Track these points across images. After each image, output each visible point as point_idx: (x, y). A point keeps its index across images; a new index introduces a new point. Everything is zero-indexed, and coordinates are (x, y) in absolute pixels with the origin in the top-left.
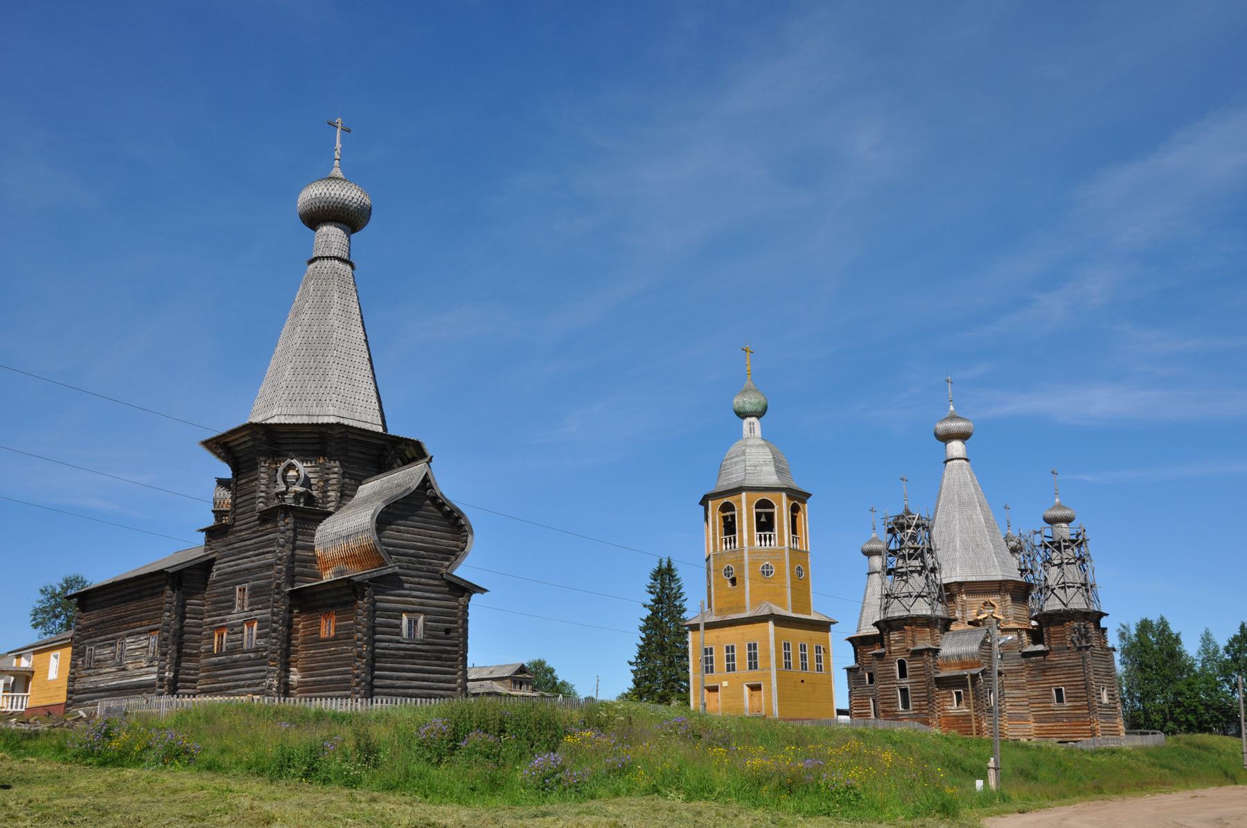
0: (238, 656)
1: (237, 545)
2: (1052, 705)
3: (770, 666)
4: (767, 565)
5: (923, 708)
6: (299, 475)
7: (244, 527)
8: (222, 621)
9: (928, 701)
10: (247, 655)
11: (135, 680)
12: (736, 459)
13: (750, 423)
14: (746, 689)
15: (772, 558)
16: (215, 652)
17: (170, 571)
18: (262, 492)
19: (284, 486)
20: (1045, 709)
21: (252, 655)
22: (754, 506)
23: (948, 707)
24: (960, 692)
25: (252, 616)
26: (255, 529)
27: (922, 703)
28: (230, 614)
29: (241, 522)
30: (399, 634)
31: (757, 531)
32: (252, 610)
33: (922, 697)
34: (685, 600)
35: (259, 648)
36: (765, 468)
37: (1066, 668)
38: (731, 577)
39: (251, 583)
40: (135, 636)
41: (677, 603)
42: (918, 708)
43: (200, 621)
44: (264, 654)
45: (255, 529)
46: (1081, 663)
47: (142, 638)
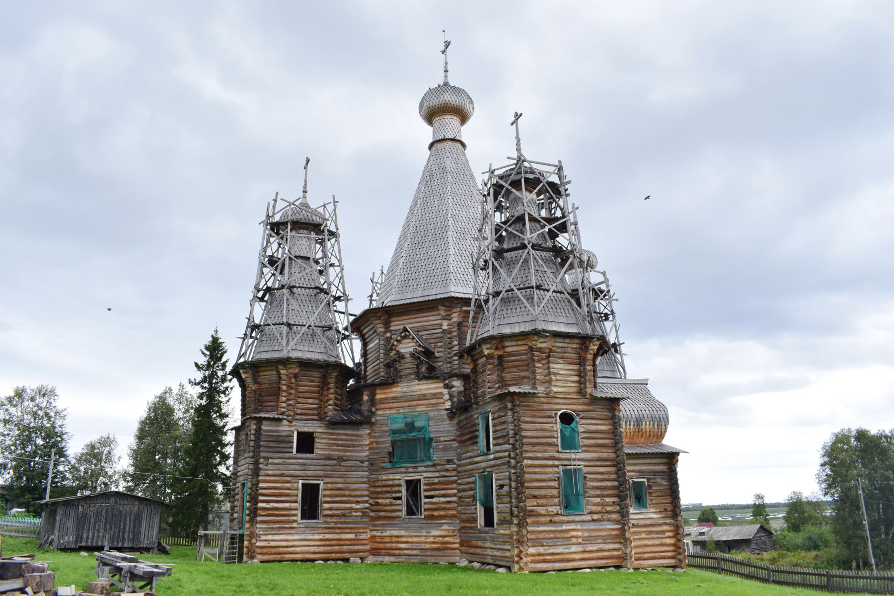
5: (609, 508)
27: (607, 500)
33: (605, 488)
42: (599, 508)
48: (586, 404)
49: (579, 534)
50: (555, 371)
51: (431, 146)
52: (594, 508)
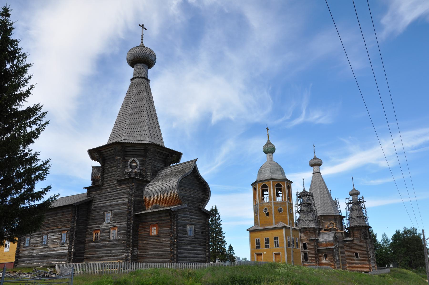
0: (107, 243)
1: (105, 194)
2: (354, 259)
3: (284, 246)
4: (280, 208)
5: (313, 260)
6: (137, 165)
7: (109, 187)
8: (97, 227)
9: (315, 258)
10: (113, 242)
11: (54, 252)
12: (266, 169)
13: (270, 156)
14: (274, 255)
15: (282, 205)
16: (94, 241)
17: (75, 205)
18: (119, 172)
19: (130, 169)
20: (352, 260)
21: (115, 242)
22: (275, 186)
23: (322, 260)
24: (326, 254)
25: (115, 225)
26: (114, 188)
27: (313, 258)
28: (101, 224)
29: (107, 185)
30: (186, 234)
31: (276, 195)
32: (114, 223)
33: (312, 256)
34: (221, 221)
35: (120, 239)
36: (278, 172)
37: (359, 246)
38: (267, 212)
39: (113, 211)
40: (53, 233)
41: (218, 222)
42: (311, 260)
43: (85, 227)
44: (123, 242)
45: (114, 188)
46: (365, 244)
47: (57, 234)
48: (308, 241)
49: (307, 265)
50: (302, 235)
51: (313, 174)
52: (310, 260)
